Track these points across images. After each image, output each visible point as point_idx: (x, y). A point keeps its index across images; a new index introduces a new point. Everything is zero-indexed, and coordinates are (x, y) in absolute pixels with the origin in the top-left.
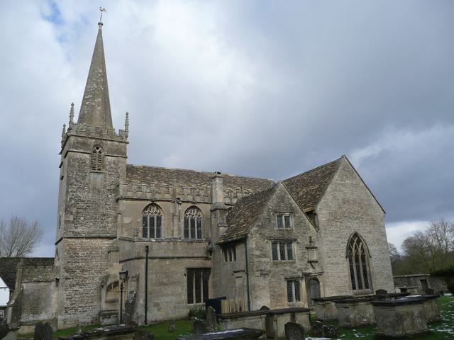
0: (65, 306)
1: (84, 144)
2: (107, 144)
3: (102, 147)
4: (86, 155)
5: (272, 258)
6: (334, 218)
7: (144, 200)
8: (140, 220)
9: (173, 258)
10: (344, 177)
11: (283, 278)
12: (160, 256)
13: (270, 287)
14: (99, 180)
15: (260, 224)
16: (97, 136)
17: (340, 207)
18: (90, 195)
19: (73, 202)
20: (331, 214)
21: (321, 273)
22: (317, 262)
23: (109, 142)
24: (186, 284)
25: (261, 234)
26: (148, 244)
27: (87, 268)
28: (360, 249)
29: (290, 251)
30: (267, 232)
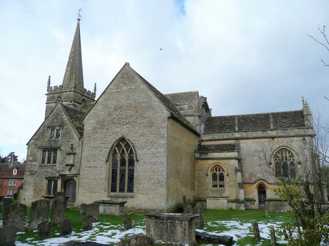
6: (101, 125)
11: (44, 177)
13: (35, 184)
17: (110, 114)
20: (98, 123)
23: (64, 93)
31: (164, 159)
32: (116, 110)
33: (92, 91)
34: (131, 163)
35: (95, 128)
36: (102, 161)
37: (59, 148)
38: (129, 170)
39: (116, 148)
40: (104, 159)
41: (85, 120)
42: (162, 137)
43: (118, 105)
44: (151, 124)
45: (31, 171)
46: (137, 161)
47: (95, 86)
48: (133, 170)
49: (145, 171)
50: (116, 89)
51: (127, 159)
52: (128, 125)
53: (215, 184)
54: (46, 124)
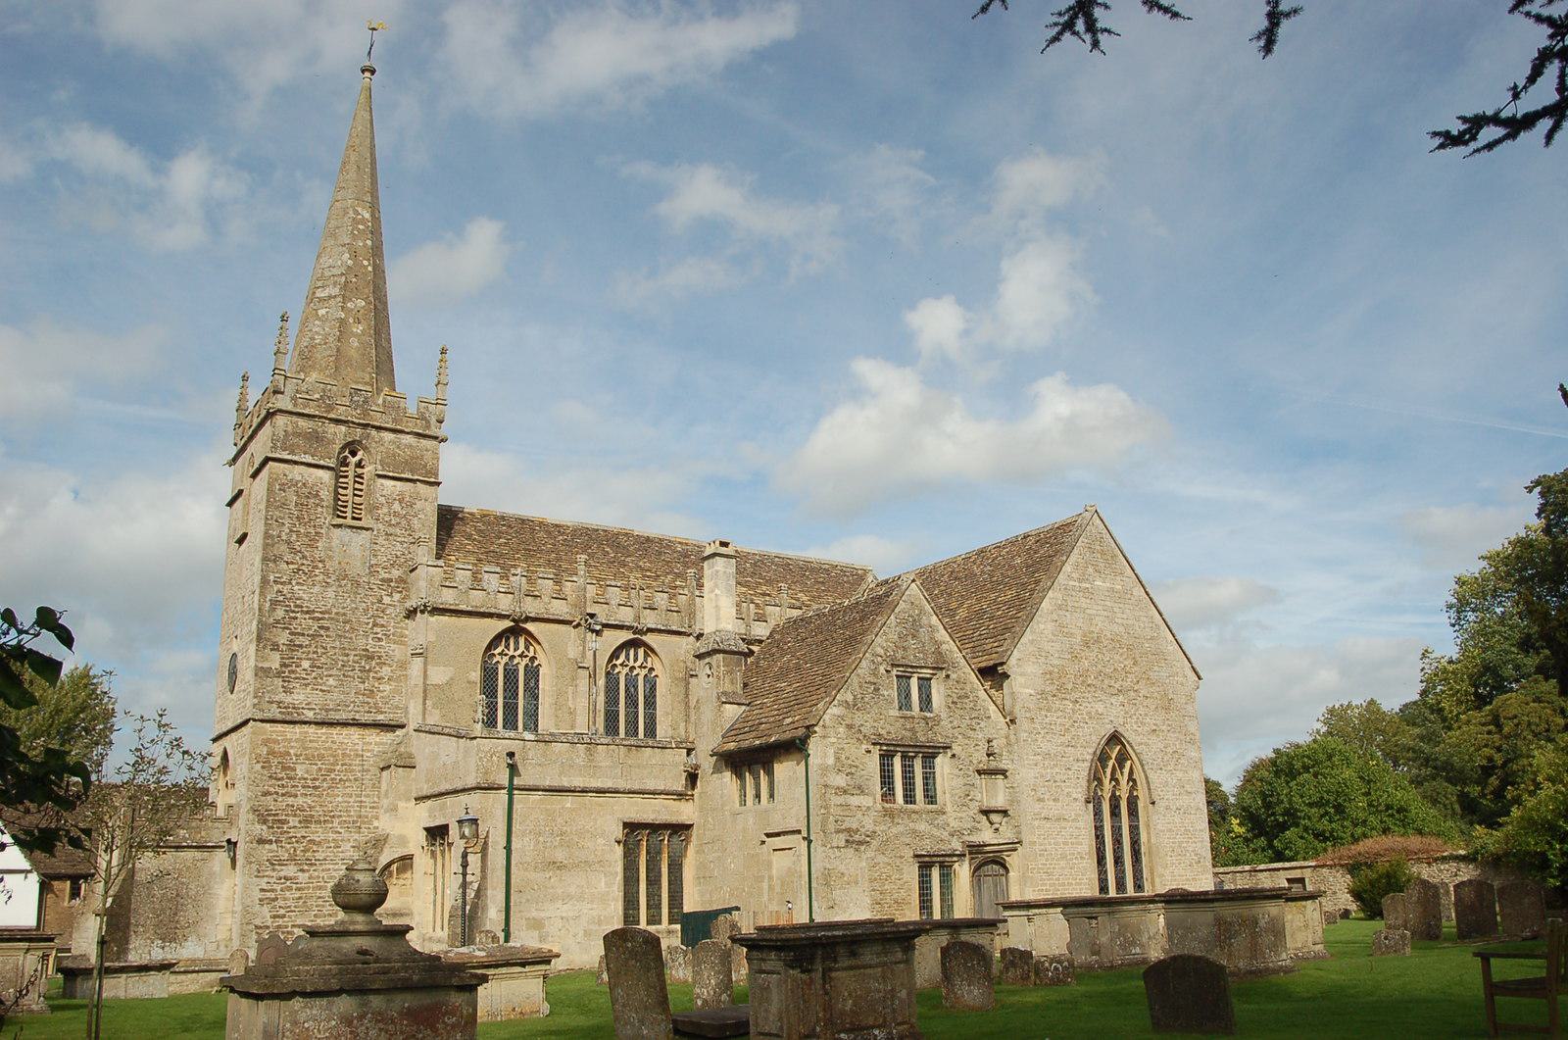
0: (258, 922)
1: (316, 438)
2: (381, 442)
3: (365, 449)
4: (320, 473)
5: (879, 797)
6: (1057, 687)
7: (490, 615)
8: (476, 675)
9: (584, 791)
10: (1091, 570)
12: (547, 783)
13: (871, 881)
15: (850, 698)
16: (353, 415)
18: (330, 592)
19: (280, 613)
21: (1014, 845)
22: (1005, 813)
23: (388, 436)
24: (620, 868)
25: (850, 727)
26: (514, 746)
27: (317, 812)
28: (1124, 780)
29: (929, 778)
30: (867, 722)
45: (848, 830)
49: (1170, 830)
50: (1080, 581)
54: (881, 651)
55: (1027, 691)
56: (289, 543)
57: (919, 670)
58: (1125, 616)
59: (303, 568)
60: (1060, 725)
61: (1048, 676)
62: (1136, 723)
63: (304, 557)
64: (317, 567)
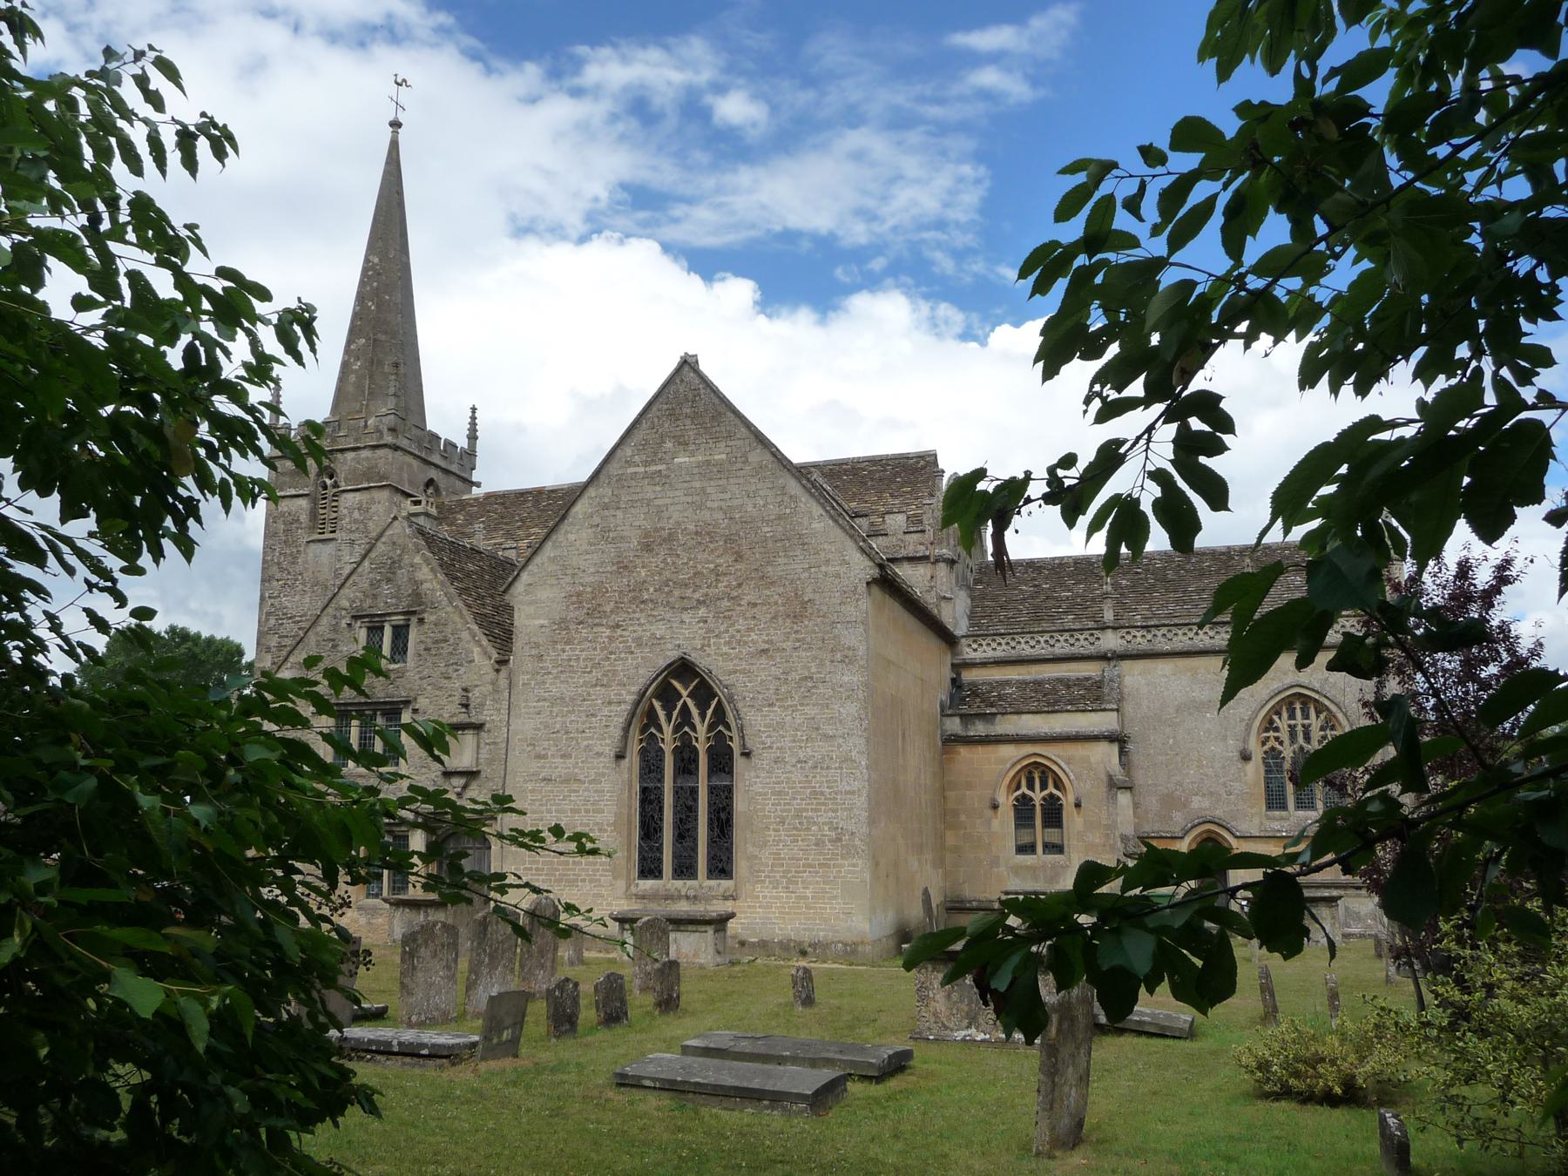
10: (669, 445)
14: (325, 559)
17: (623, 567)
18: (307, 600)
19: (272, 622)
31: (856, 746)
32: (647, 547)
33: (462, 443)
34: (722, 761)
35: (563, 620)
36: (599, 754)
37: (407, 703)
38: (712, 790)
39: (657, 705)
40: (608, 747)
41: (519, 587)
42: (848, 660)
43: (656, 530)
44: (798, 610)
46: (747, 754)
47: (473, 418)
48: (729, 790)
50: (646, 464)
51: (702, 747)
52: (702, 612)
53: (1026, 839)
54: (346, 604)
55: (537, 622)
56: (279, 564)
57: (388, 619)
58: (728, 496)
59: (289, 582)
60: (584, 660)
61: (574, 599)
62: (728, 643)
63: (289, 573)
64: (296, 580)
